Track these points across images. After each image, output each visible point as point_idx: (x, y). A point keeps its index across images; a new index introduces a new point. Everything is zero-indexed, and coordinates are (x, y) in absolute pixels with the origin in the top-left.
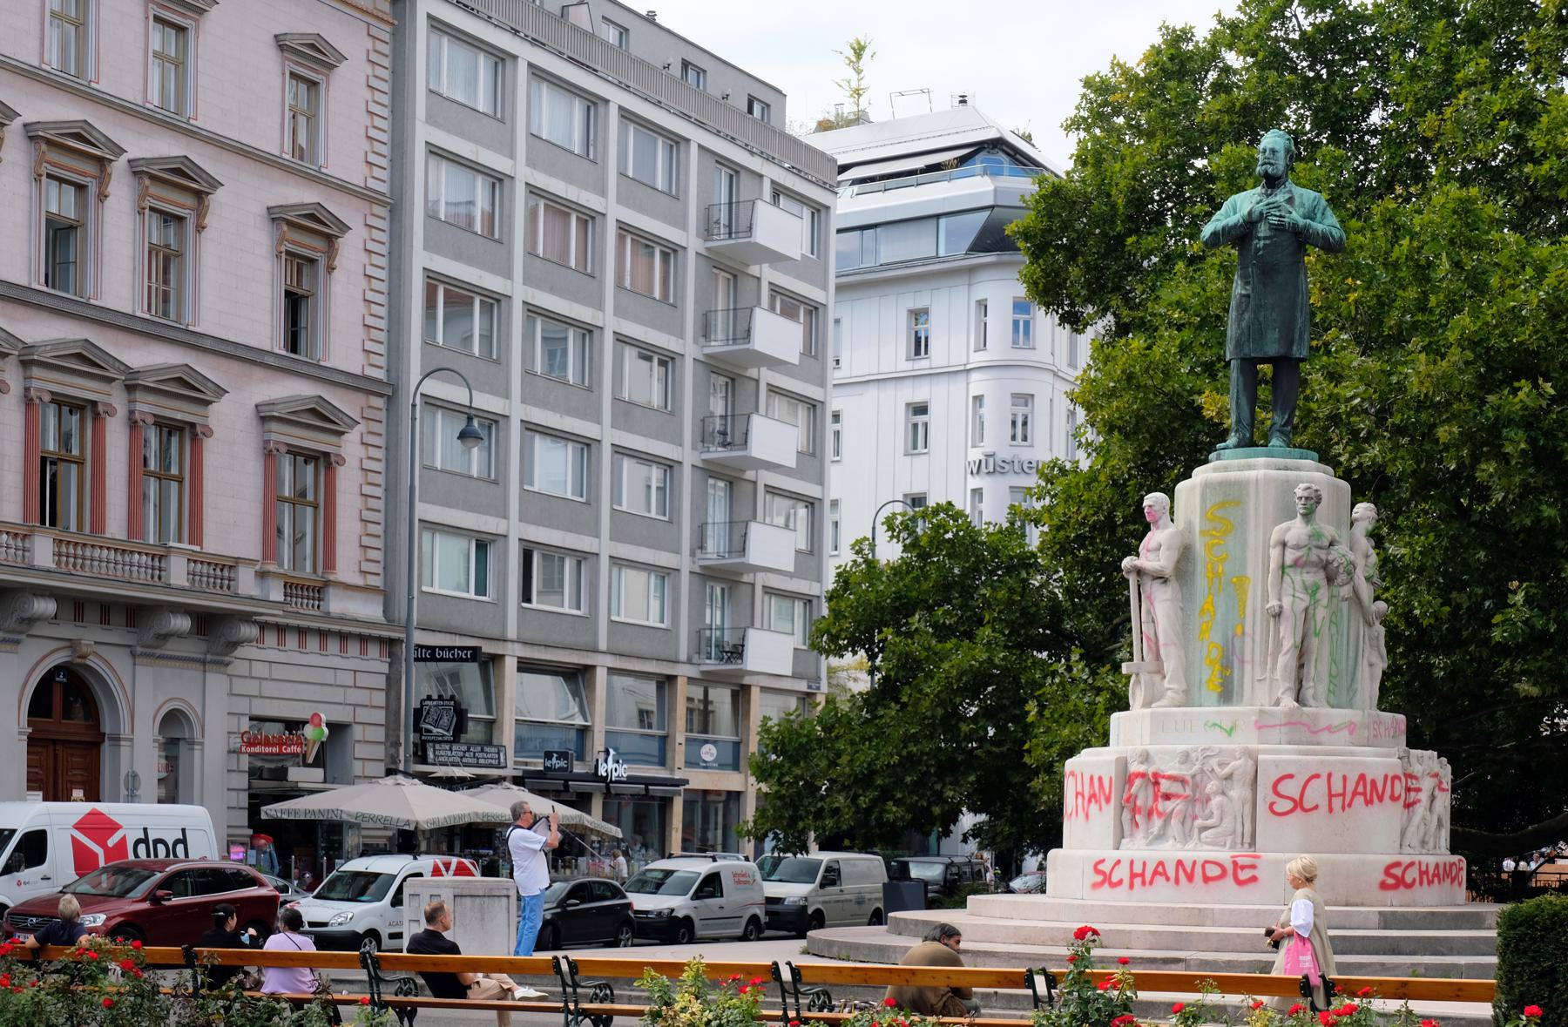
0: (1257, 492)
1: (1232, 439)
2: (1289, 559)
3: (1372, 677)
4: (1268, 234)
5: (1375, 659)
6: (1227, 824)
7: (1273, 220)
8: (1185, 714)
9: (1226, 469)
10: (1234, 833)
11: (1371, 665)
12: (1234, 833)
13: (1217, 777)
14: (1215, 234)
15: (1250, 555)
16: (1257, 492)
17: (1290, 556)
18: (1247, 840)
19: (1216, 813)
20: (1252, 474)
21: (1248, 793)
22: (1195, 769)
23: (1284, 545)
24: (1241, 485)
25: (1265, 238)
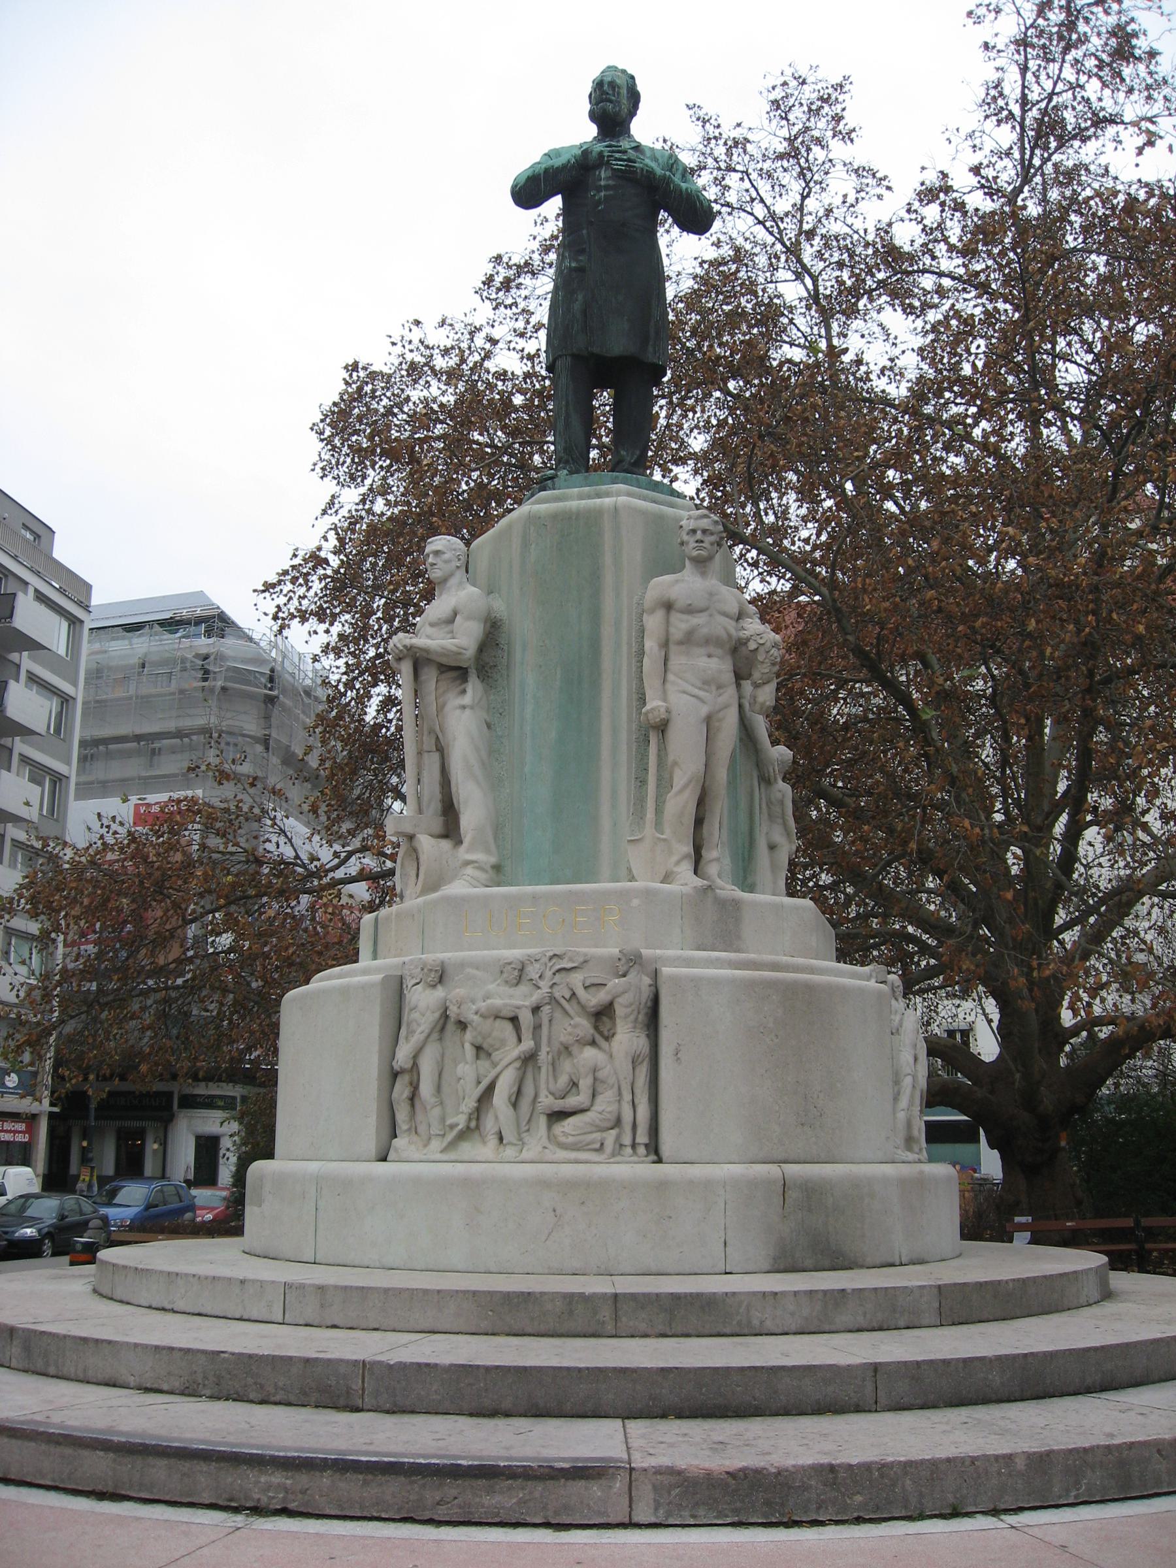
3: (774, 867)
4: (611, 182)
5: (778, 837)
6: (605, 1105)
7: (619, 165)
8: (506, 897)
10: (618, 1122)
11: (772, 847)
12: (618, 1122)
15: (607, 630)
18: (642, 1138)
19: (585, 1083)
20: (607, 501)
21: (641, 1043)
22: (536, 997)
24: (590, 521)
25: (607, 188)
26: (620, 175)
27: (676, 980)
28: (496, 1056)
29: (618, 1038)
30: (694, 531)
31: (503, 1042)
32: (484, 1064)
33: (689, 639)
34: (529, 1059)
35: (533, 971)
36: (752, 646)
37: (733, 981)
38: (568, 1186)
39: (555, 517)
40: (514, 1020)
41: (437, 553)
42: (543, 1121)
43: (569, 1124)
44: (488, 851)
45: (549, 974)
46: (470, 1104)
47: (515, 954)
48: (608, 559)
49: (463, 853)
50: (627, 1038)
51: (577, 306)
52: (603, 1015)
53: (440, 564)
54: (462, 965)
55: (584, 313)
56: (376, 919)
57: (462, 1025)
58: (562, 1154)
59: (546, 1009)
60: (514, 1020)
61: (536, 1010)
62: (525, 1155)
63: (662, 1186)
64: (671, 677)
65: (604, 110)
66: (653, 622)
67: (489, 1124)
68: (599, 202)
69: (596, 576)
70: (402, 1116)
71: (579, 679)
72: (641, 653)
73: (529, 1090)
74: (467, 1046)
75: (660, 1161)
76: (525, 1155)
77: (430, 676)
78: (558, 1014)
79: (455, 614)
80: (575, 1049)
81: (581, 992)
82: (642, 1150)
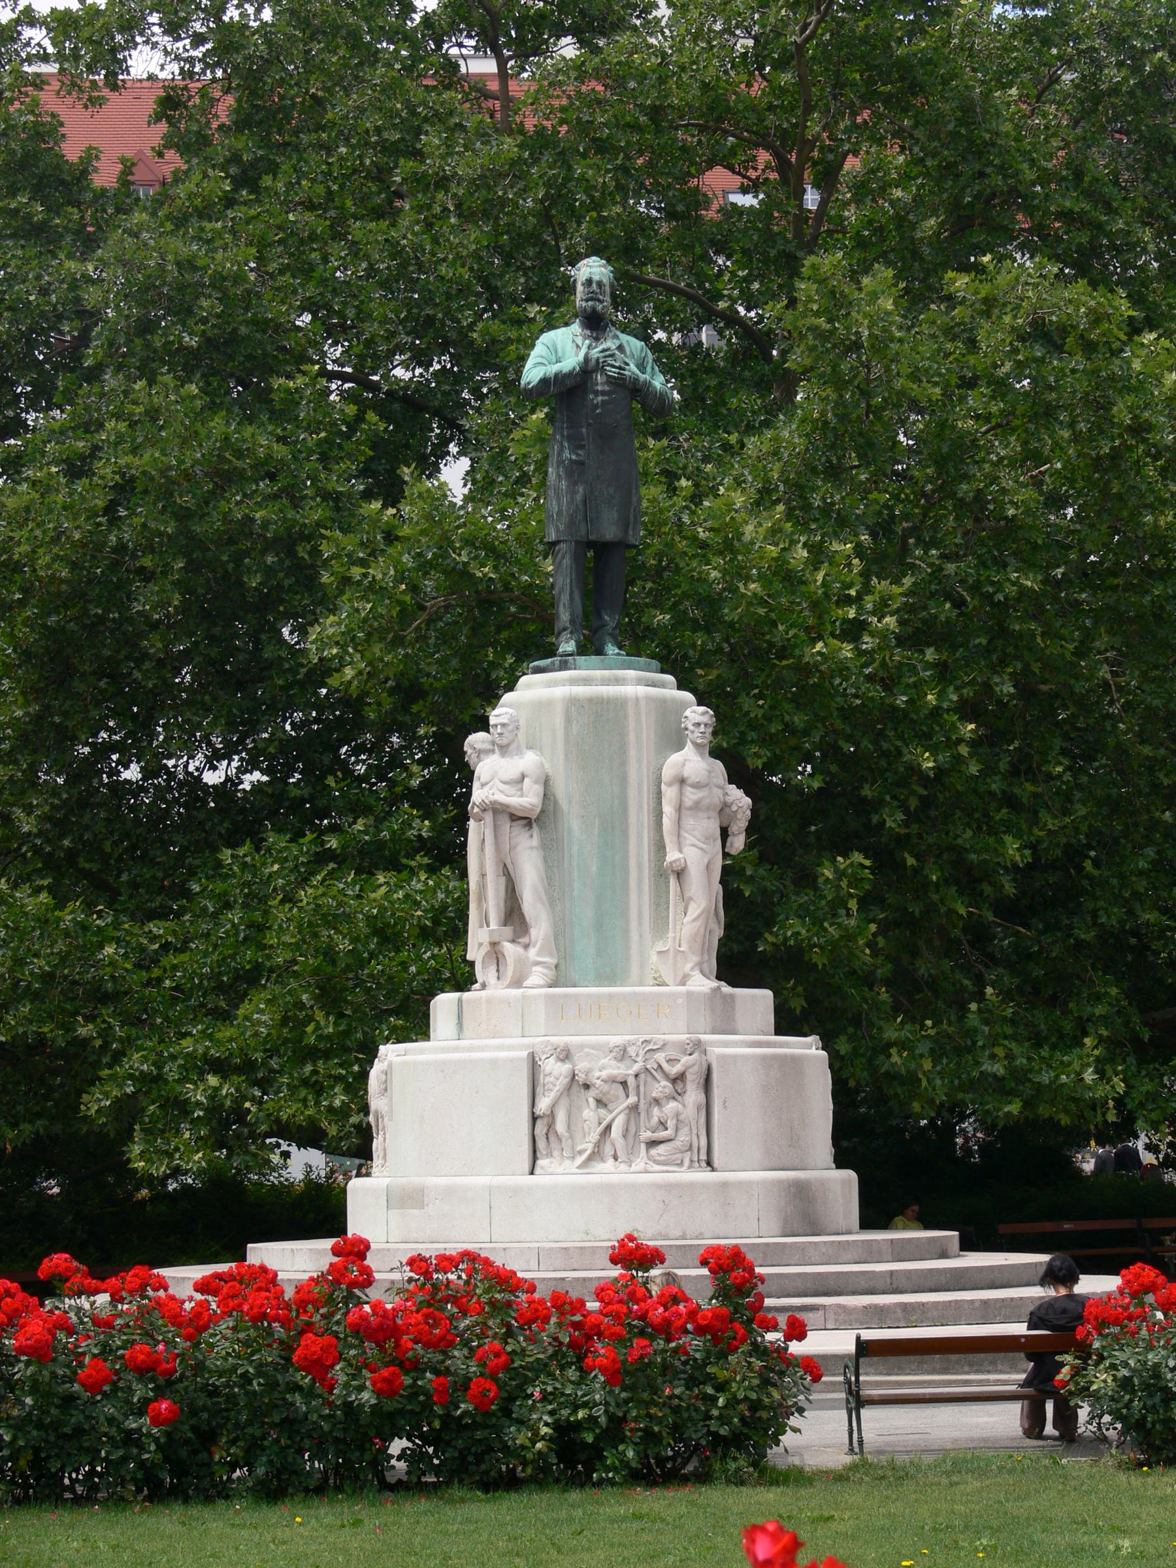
0: (638, 714)
1: (568, 646)
2: (688, 802)
4: (607, 388)
6: (683, 1137)
7: (612, 372)
9: (586, 682)
10: (690, 1148)
12: (690, 1148)
13: (666, 1076)
14: (544, 381)
15: (632, 793)
16: (638, 714)
17: (691, 796)
18: (704, 1157)
19: (671, 1124)
21: (702, 1097)
22: (636, 1068)
23: (682, 781)
24: (619, 704)
25: (603, 393)
26: (610, 380)
27: (723, 1058)
28: (610, 1106)
29: (688, 1093)
30: (699, 724)
31: (617, 1098)
32: (602, 1111)
33: (696, 806)
34: (634, 1109)
35: (632, 1051)
36: (734, 808)
37: (755, 1056)
38: (669, 1187)
39: (591, 700)
40: (624, 1084)
41: (503, 725)
42: (643, 1146)
43: (661, 1149)
44: (551, 955)
45: (642, 1053)
46: (594, 1136)
47: (617, 1040)
48: (632, 737)
49: (532, 953)
50: (694, 1095)
51: (579, 497)
52: (678, 1079)
53: (506, 734)
54: (582, 1047)
55: (585, 502)
56: (460, 1000)
57: (587, 1087)
58: (657, 1168)
59: (642, 1076)
60: (624, 1084)
61: (636, 1076)
62: (633, 1168)
63: (725, 1185)
64: (684, 834)
65: (594, 309)
66: (669, 793)
67: (608, 1149)
68: (597, 406)
69: (623, 749)
70: (541, 1144)
71: (613, 825)
72: (659, 814)
73: (632, 1129)
74: (591, 1100)
75: (713, 1170)
76: (633, 1168)
77: (506, 825)
78: (649, 1079)
79: (523, 777)
80: (663, 1102)
81: (665, 1066)
82: (704, 1164)
